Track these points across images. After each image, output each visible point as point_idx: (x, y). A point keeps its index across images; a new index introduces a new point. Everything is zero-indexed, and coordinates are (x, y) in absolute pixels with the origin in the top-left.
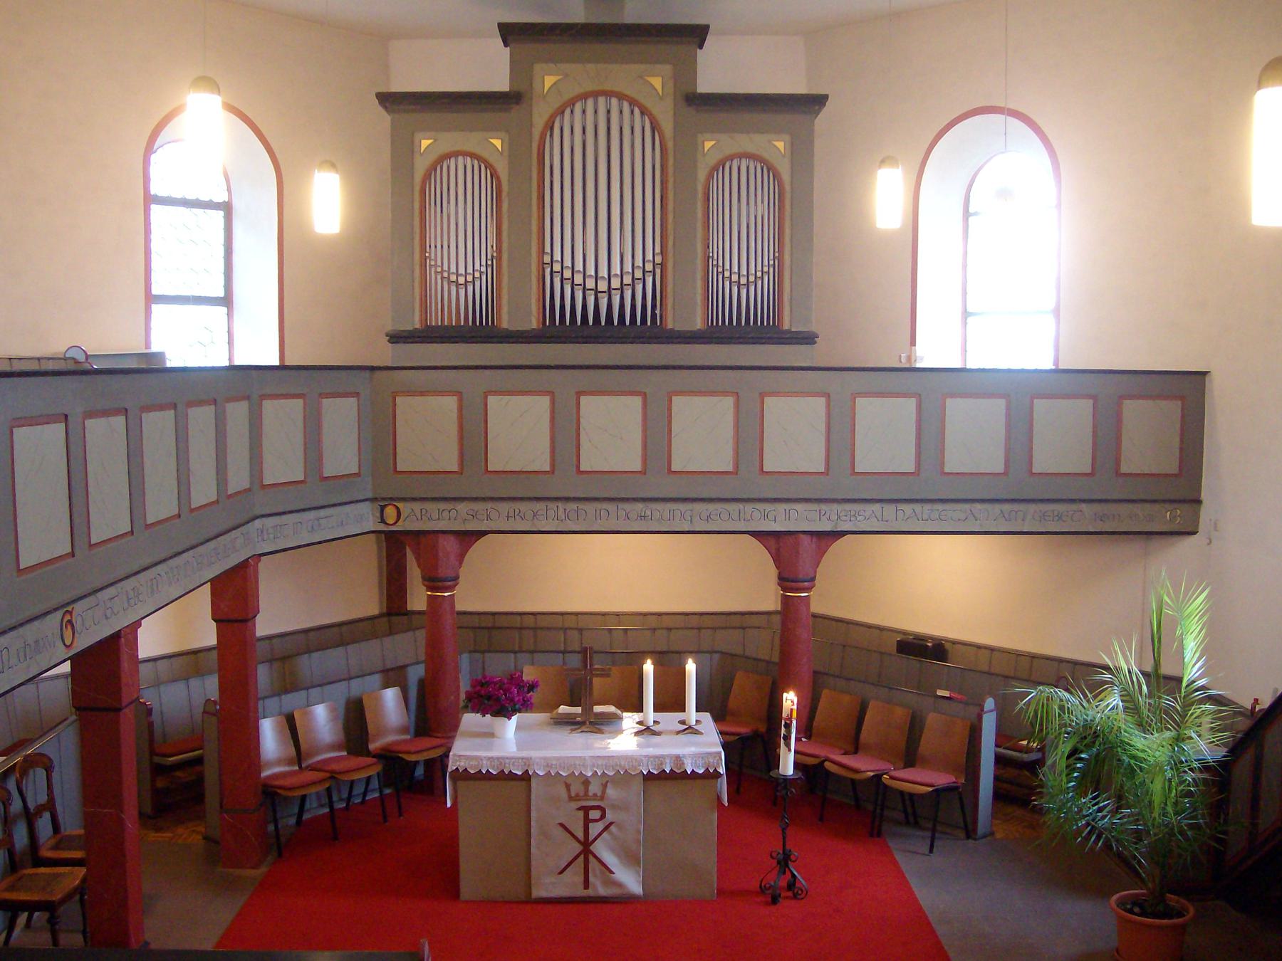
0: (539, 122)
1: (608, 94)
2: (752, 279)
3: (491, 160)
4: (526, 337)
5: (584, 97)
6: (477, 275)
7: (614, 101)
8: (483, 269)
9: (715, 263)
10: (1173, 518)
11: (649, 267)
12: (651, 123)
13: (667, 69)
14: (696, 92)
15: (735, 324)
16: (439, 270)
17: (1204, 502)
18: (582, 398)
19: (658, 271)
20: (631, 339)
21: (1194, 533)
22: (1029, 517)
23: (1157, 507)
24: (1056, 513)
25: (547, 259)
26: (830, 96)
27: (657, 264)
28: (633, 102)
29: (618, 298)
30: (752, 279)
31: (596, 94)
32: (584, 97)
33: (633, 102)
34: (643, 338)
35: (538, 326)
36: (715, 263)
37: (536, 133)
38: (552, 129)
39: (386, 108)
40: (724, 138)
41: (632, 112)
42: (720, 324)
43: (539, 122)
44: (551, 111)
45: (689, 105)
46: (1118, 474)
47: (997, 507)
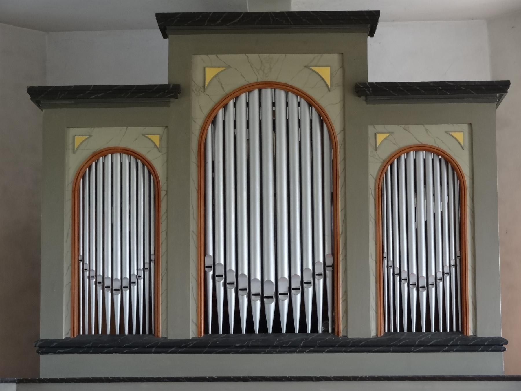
1: (275, 85)
2: (432, 280)
3: (149, 157)
4: (185, 347)
5: (248, 89)
6: (134, 279)
8: (141, 274)
9: (391, 264)
11: (319, 269)
12: (320, 116)
13: (334, 58)
15: (414, 330)
16: (93, 274)
19: (329, 273)
20: (300, 348)
25: (209, 262)
26: (511, 82)
27: (328, 266)
29: (286, 302)
30: (432, 280)
31: (262, 86)
32: (248, 89)
33: (299, 94)
36: (391, 264)
37: (196, 129)
38: (214, 123)
39: (38, 103)
40: (397, 129)
41: (299, 104)
42: (398, 330)
44: (211, 105)
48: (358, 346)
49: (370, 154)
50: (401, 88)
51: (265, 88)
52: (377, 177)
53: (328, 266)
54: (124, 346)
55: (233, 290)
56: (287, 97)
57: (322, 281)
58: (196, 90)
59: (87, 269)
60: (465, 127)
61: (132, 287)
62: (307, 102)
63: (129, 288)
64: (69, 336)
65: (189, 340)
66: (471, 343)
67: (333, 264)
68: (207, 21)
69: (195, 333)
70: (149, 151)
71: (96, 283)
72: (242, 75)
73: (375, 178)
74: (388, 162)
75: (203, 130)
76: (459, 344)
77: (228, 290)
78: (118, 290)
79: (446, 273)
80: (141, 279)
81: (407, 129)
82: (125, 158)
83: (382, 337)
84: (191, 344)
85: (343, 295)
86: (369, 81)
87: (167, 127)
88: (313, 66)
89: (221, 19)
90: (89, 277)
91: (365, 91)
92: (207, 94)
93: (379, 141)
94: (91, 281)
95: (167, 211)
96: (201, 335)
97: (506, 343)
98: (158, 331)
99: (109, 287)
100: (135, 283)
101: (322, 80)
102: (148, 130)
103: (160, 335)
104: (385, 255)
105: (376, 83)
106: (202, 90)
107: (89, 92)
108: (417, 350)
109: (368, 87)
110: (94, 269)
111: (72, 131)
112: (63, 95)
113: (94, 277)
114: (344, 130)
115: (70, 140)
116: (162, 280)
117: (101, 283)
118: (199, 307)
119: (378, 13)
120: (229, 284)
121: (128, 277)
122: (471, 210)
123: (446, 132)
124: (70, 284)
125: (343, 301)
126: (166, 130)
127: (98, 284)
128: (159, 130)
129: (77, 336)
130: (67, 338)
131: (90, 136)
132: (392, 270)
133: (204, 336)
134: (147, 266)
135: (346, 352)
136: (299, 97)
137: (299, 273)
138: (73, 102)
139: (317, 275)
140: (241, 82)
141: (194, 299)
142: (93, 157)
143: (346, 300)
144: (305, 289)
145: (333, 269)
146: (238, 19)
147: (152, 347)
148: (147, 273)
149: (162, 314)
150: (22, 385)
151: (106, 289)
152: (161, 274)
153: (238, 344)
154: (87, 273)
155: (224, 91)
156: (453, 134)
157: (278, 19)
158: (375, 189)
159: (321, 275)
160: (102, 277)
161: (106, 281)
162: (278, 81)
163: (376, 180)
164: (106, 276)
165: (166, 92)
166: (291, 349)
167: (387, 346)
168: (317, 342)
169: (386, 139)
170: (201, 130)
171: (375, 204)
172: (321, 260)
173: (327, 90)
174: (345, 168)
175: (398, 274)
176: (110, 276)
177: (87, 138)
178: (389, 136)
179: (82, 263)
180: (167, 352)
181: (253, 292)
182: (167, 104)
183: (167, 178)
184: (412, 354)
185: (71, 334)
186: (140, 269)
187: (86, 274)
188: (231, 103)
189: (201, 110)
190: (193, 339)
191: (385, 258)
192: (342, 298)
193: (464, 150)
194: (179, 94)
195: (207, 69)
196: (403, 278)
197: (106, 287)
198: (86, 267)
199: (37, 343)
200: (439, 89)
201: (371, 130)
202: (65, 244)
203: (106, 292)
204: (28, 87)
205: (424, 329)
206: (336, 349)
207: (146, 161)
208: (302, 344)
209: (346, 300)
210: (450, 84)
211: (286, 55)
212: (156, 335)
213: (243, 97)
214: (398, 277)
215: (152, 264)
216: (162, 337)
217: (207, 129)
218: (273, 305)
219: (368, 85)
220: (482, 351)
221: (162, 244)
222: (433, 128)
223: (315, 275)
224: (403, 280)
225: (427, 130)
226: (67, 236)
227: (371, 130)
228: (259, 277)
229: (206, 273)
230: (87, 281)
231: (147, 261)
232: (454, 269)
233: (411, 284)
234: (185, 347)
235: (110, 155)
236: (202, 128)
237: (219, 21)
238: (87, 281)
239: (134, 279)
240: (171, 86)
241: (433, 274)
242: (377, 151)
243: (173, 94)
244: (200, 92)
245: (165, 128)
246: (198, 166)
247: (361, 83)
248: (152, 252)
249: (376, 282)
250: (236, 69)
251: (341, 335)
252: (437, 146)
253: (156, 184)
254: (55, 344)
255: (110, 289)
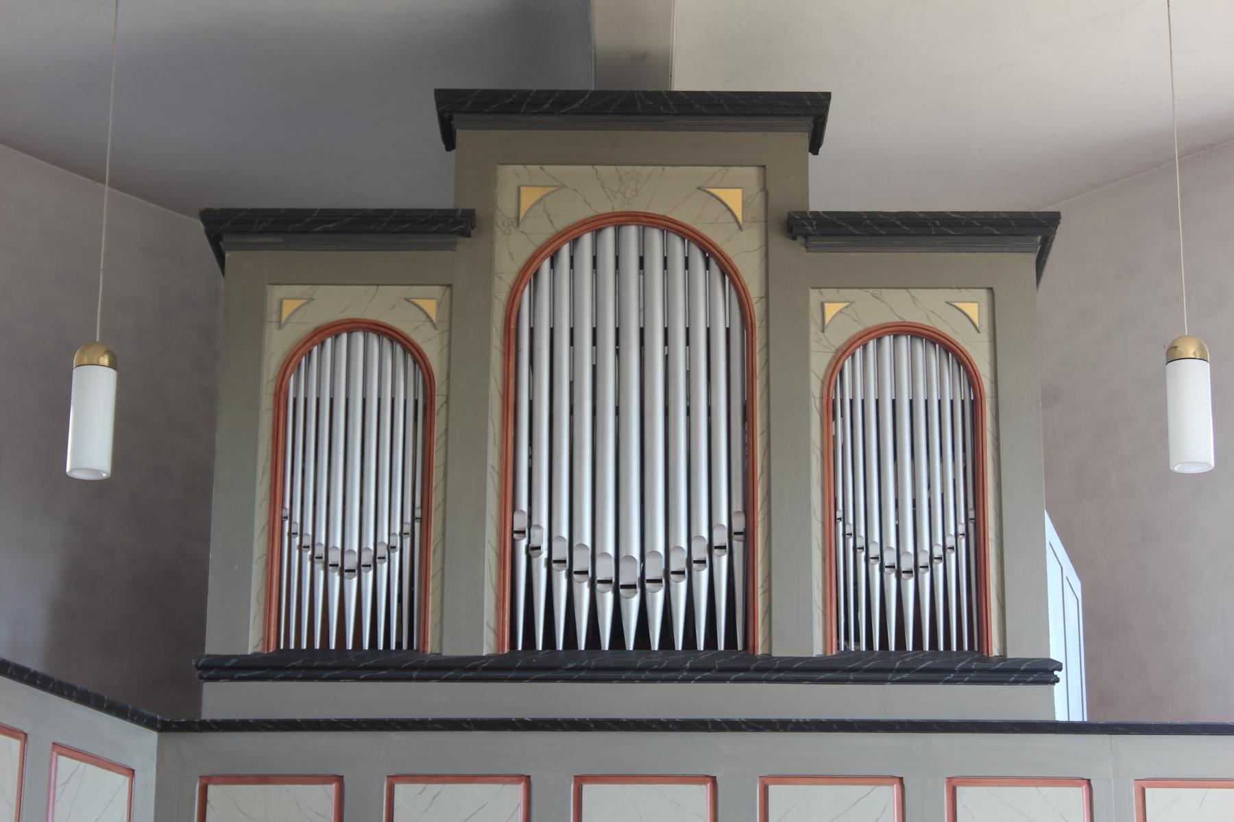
0: (507, 268)
1: (645, 221)
2: (924, 559)
3: (417, 337)
4: (474, 668)
5: (596, 226)
6: (382, 551)
7: (655, 236)
8: (396, 541)
11: (721, 538)
13: (753, 172)
14: (805, 212)
16: (307, 541)
18: (588, 789)
19: (738, 546)
20: (685, 674)
25: (520, 522)
27: (736, 533)
28: (689, 236)
31: (620, 221)
32: (596, 226)
34: (709, 670)
35: (500, 644)
36: (849, 529)
37: (502, 289)
40: (862, 297)
43: (507, 268)
44: (531, 250)
45: (794, 238)
48: (789, 670)
49: (812, 337)
50: (868, 222)
51: (627, 223)
52: (825, 377)
53: (736, 533)
54: (362, 665)
55: (563, 573)
56: (666, 245)
57: (725, 559)
58: (503, 224)
59: (296, 534)
60: (983, 295)
61: (378, 565)
62: (700, 249)
63: (372, 567)
64: (259, 649)
65: (482, 658)
66: (997, 667)
67: (745, 529)
68: (525, 104)
69: (492, 647)
70: (417, 328)
71: (312, 558)
72: (585, 200)
73: (821, 378)
74: (844, 352)
75: (515, 293)
76: (973, 667)
77: (555, 573)
78: (354, 571)
79: (949, 548)
80: (396, 551)
81: (878, 296)
82: (374, 340)
83: (833, 656)
84: (483, 663)
85: (764, 581)
86: (812, 209)
87: (450, 286)
88: (713, 188)
89: (550, 101)
90: (300, 547)
91: (804, 225)
92: (522, 232)
93: (828, 318)
94: (304, 553)
95: (446, 430)
96: (503, 650)
97: (1059, 667)
98: (425, 643)
99: (337, 565)
100: (384, 558)
101: (728, 212)
102: (416, 290)
103: (429, 650)
104: (839, 514)
105: (823, 212)
106: (514, 225)
107: (310, 219)
108: (898, 678)
109: (809, 219)
110: (310, 532)
111: (277, 292)
112: (264, 224)
113: (308, 547)
114: (766, 296)
115: (272, 306)
116: (434, 552)
117: (321, 558)
118: (500, 600)
119: (827, 96)
120: (557, 562)
121: (371, 547)
122: (993, 436)
123: (947, 302)
124: (265, 558)
125: (764, 592)
126: (448, 289)
127: (316, 560)
128: (437, 291)
129: (274, 652)
130: (255, 654)
131: (311, 300)
132: (851, 541)
133: (508, 653)
134: (407, 529)
135: (768, 681)
136: (686, 241)
137: (684, 545)
138: (280, 239)
139: (717, 547)
140: (586, 213)
141: (492, 586)
142: (314, 336)
143: (768, 591)
144: (694, 573)
145: (745, 537)
146: (581, 102)
147: (412, 668)
148: (407, 541)
149: (432, 612)
150: (166, 735)
151: (330, 568)
152: (434, 542)
153: (571, 663)
154: (297, 540)
155: (553, 226)
156: (959, 305)
157: (651, 103)
158: (822, 398)
159: (724, 547)
160: (324, 547)
161: (331, 554)
162: (649, 211)
163: (823, 383)
164: (331, 545)
165: (450, 221)
166: (669, 675)
167: (844, 670)
168: (717, 662)
169: (840, 312)
170: (511, 292)
171: (822, 424)
172: (725, 522)
173: (737, 227)
174: (767, 361)
175: (862, 548)
176: (339, 545)
177: (305, 303)
178: (847, 307)
179: (287, 522)
180: (440, 680)
181: (599, 578)
182: (451, 246)
183: (448, 374)
184: (889, 687)
185: (264, 645)
186: (395, 534)
187: (295, 542)
188: (565, 250)
189: (512, 258)
190: (488, 657)
191: (840, 519)
192: (762, 586)
193: (979, 332)
194: (472, 229)
195: (523, 190)
196: (872, 554)
197: (331, 565)
198: (296, 528)
199: (199, 660)
200: (935, 225)
201: (814, 296)
202: (258, 487)
203: (330, 573)
204: (202, 209)
205: (910, 647)
206: (750, 675)
207: (411, 344)
208: (688, 665)
209: (768, 591)
210: (953, 215)
211: (664, 169)
212: (421, 649)
213: (587, 239)
214: (863, 554)
215: (417, 525)
216: (432, 654)
217: (522, 292)
218: (635, 601)
219: (810, 216)
220: (1016, 682)
221: (436, 488)
222: (925, 296)
223: (713, 548)
224: (872, 558)
225: (913, 298)
226: (263, 473)
227: (814, 296)
228: (610, 549)
229: (514, 542)
230: (296, 553)
231: (408, 518)
232: (963, 541)
233: (887, 567)
234: (474, 668)
235: (344, 336)
236: (512, 289)
237: (547, 105)
238: (297, 552)
239: (382, 551)
240: (460, 212)
241: (927, 548)
242: (825, 332)
243: (462, 227)
244: (511, 227)
245: (445, 288)
246: (504, 354)
247: (796, 213)
248: (418, 503)
249: (824, 560)
250: (575, 190)
251: (760, 651)
252: (930, 324)
253: (428, 383)
254: (233, 661)
255: (339, 568)
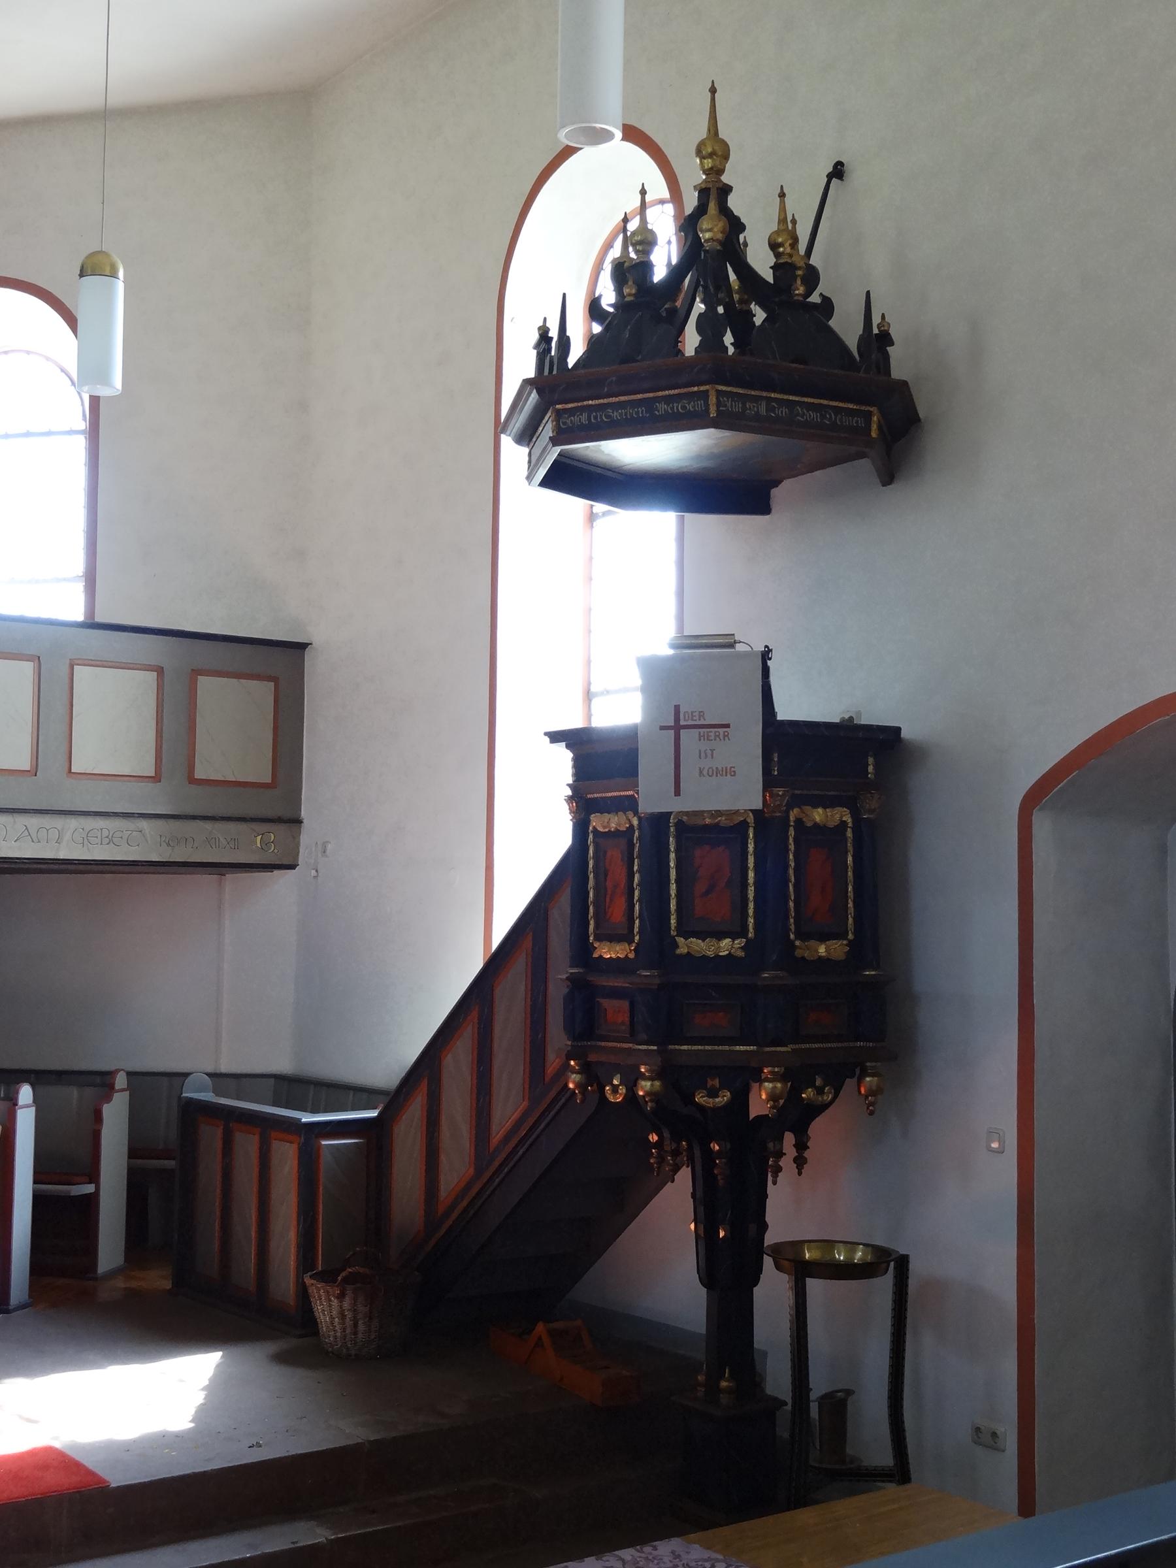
10: (266, 844)
17: (305, 821)
21: (292, 867)
22: (67, 837)
23: (243, 827)
24: (105, 833)
46: (192, 780)
47: (22, 820)
